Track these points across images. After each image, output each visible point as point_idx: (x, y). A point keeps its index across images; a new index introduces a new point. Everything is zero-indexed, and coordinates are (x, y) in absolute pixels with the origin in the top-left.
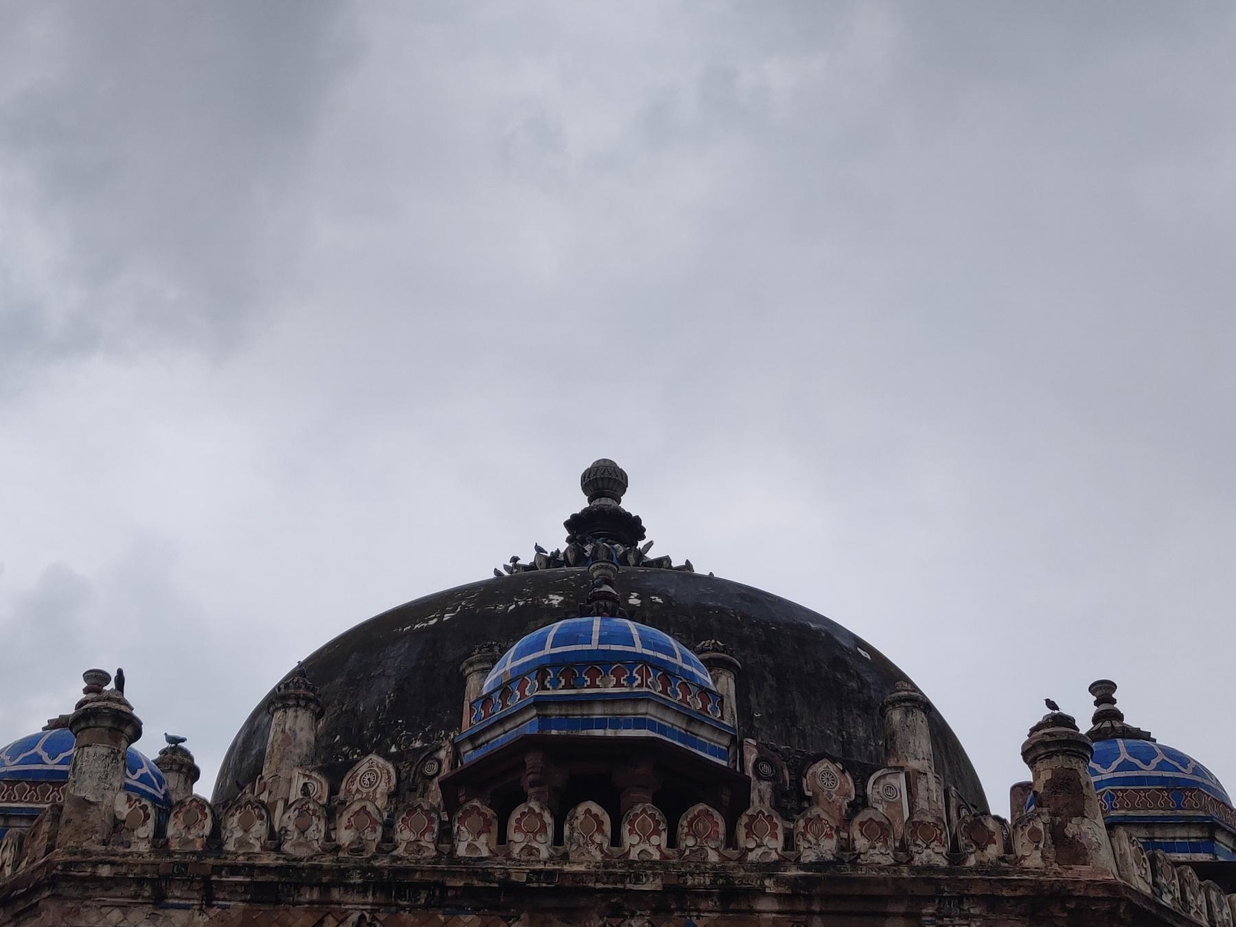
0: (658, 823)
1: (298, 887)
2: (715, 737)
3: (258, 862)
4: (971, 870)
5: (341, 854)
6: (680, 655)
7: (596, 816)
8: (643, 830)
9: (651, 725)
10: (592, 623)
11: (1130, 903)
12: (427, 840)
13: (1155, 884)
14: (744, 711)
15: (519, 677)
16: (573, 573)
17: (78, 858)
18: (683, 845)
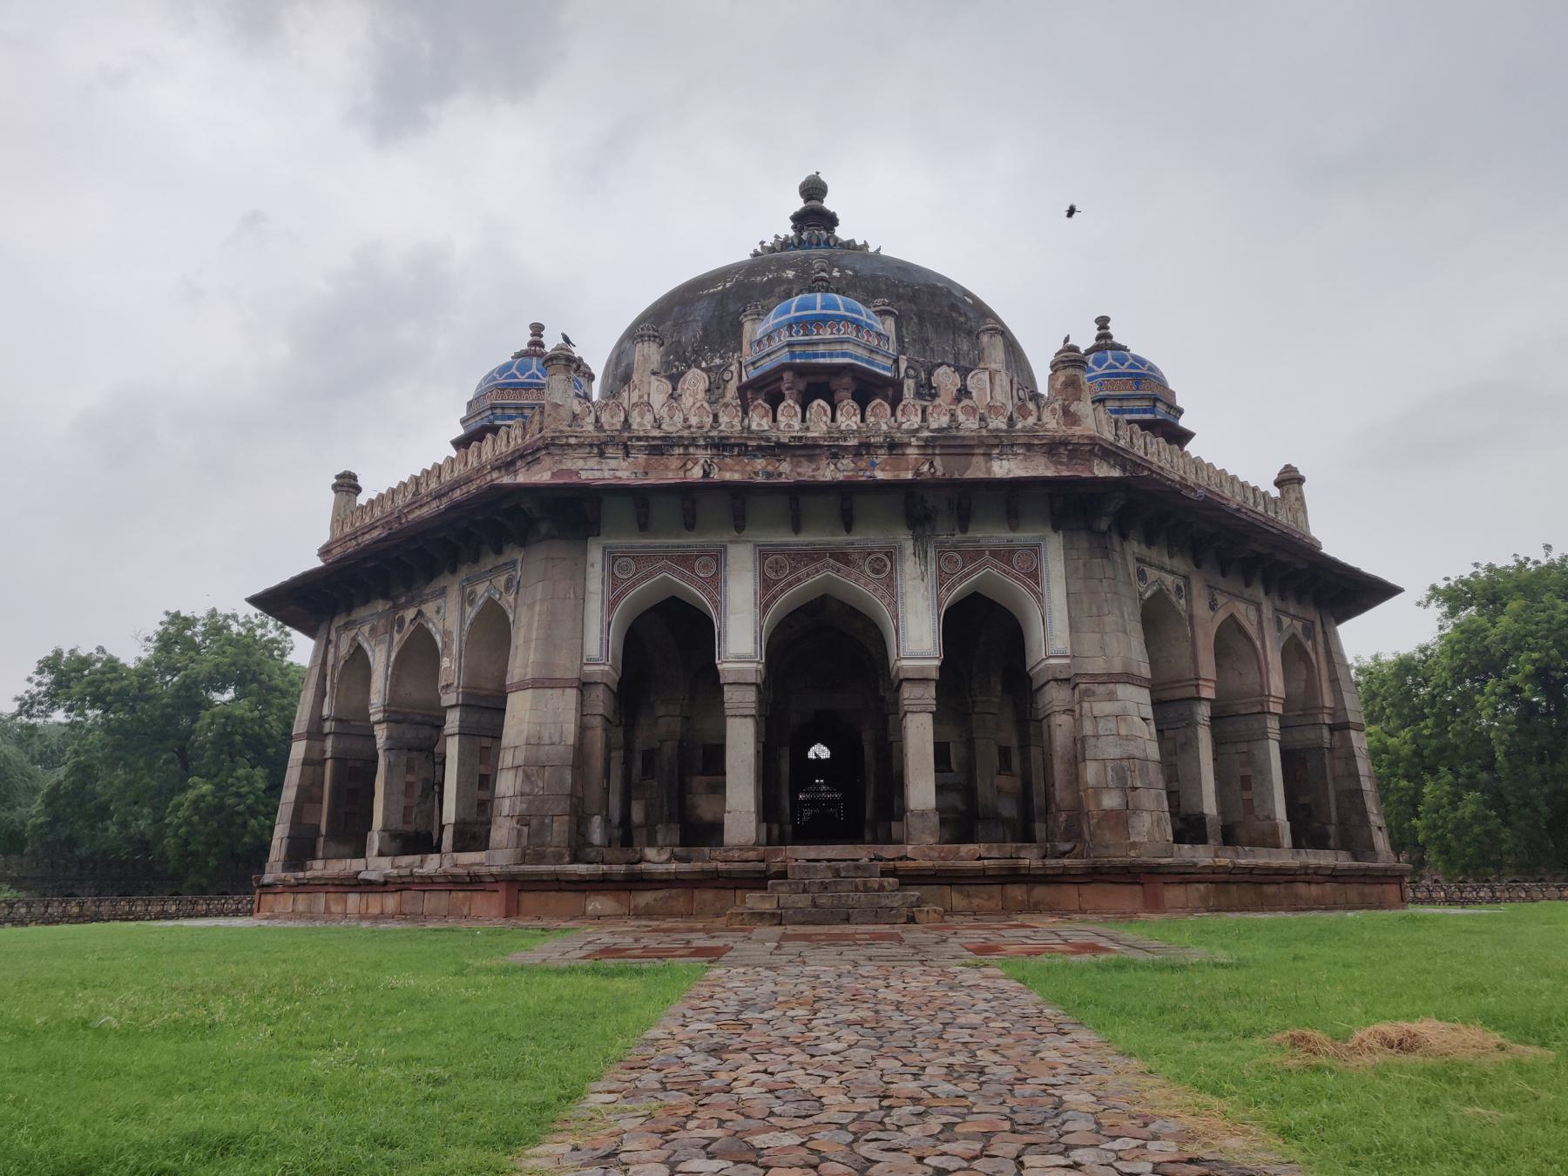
0: (855, 410)
1: (672, 446)
2: (885, 360)
3: (651, 435)
4: (1019, 431)
6: (866, 314)
7: (823, 407)
8: (848, 413)
9: (851, 356)
10: (816, 298)
11: (1101, 446)
12: (736, 422)
13: (1117, 435)
14: (900, 339)
15: (777, 329)
16: (799, 256)
17: (558, 434)
18: (868, 421)
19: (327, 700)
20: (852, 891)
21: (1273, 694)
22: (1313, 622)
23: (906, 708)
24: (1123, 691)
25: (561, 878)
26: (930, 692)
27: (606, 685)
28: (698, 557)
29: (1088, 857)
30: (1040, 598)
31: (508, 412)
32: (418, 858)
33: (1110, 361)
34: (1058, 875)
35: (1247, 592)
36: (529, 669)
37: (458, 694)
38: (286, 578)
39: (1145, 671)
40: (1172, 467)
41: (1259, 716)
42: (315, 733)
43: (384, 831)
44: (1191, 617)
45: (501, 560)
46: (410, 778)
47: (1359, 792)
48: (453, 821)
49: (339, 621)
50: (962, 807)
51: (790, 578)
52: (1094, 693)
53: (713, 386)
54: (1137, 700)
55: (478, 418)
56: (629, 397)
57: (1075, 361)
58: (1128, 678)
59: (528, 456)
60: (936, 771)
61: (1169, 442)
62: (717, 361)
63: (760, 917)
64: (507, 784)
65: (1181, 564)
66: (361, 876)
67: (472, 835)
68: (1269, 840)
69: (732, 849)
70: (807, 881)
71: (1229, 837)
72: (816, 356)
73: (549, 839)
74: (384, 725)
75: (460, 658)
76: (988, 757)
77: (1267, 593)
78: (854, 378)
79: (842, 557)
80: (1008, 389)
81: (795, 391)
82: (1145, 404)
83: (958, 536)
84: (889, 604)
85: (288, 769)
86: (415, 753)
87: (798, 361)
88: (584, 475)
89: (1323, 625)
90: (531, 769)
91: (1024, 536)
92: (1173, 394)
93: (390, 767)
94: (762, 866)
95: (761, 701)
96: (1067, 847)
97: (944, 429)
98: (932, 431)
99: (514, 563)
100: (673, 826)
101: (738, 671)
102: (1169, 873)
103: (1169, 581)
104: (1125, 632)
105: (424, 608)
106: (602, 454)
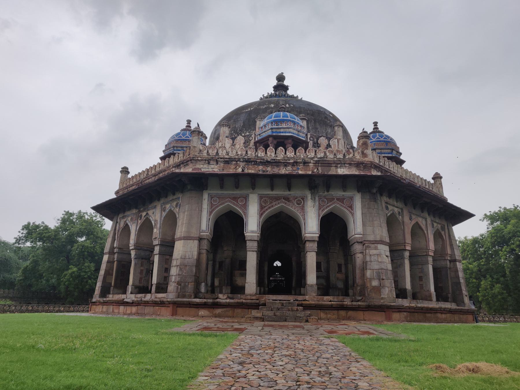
0: (293, 151)
1: (232, 161)
2: (303, 134)
3: (225, 157)
4: (347, 159)
5: (239, 156)
6: (297, 119)
7: (282, 150)
9: (292, 133)
12: (253, 153)
13: (379, 161)
14: (308, 128)
15: (268, 123)
16: (275, 100)
17: (195, 156)
18: (297, 154)
19: (116, 241)
20: (287, 311)
21: (430, 249)
22: (444, 225)
23: (307, 250)
24: (380, 246)
25: (190, 303)
26: (316, 245)
27: (208, 239)
28: (239, 198)
29: (367, 302)
30: (353, 214)
31: (178, 148)
32: (144, 295)
33: (378, 136)
34: (356, 307)
35: (422, 214)
36: (183, 233)
37: (159, 241)
38: (104, 201)
39: (387, 240)
40: (398, 172)
41: (425, 256)
42: (111, 252)
43: (133, 285)
44: (403, 222)
45: (175, 197)
46: (142, 268)
47: (459, 283)
48: (156, 283)
49: (121, 216)
50: (325, 284)
51: (270, 206)
52: (370, 247)
53: (246, 142)
54: (384, 250)
55: (169, 150)
56: (218, 145)
57: (366, 136)
58: (382, 242)
59: (184, 163)
60: (317, 272)
61: (397, 164)
62: (248, 134)
63: (256, 318)
64: (174, 271)
65: (400, 205)
66: (125, 300)
67: (162, 288)
68: (428, 298)
69: (247, 296)
70: (272, 307)
71: (415, 297)
72: (280, 132)
73: (187, 290)
74: (134, 251)
75: (160, 229)
76: (334, 267)
77: (429, 215)
78: (293, 140)
79: (287, 199)
80: (344, 145)
81: (273, 144)
82: (389, 151)
83: (326, 193)
84: (302, 215)
85: (102, 264)
86: (144, 260)
87: (274, 134)
88: (203, 170)
89: (447, 225)
90: (182, 267)
91: (348, 194)
92: (398, 148)
93: (135, 264)
94: (258, 301)
95: (259, 246)
96: (360, 298)
97: (322, 158)
98: (318, 158)
99: (179, 198)
100: (228, 287)
101: (251, 236)
102: (394, 308)
103: (396, 210)
104: (381, 227)
105: (149, 212)
106: (209, 163)
